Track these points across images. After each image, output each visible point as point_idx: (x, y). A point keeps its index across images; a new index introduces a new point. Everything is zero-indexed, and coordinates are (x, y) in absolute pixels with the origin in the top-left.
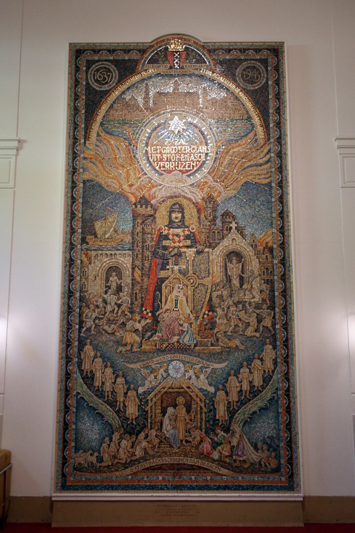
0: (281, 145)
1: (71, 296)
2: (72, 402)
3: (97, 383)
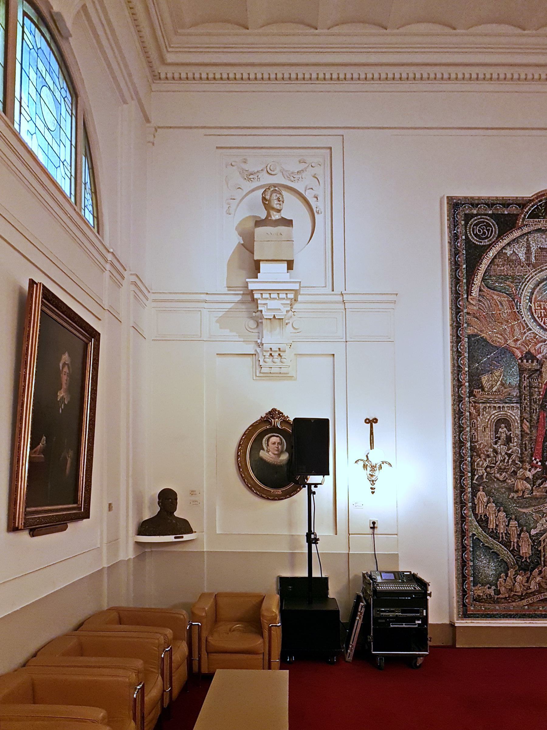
2: (468, 542)
3: (491, 526)
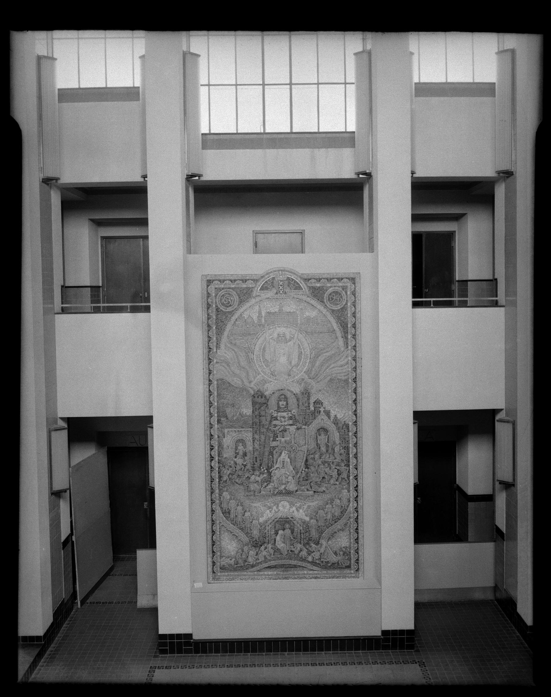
0: (356, 351)
1: (212, 460)
3: (232, 516)
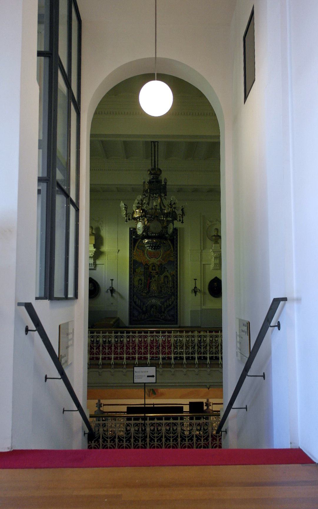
2: (132, 307)
